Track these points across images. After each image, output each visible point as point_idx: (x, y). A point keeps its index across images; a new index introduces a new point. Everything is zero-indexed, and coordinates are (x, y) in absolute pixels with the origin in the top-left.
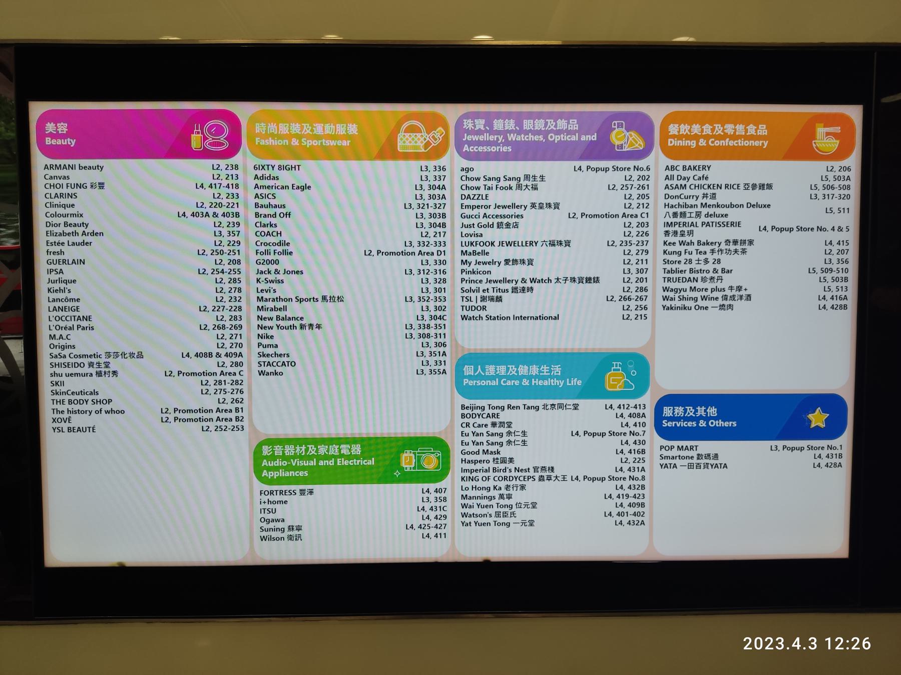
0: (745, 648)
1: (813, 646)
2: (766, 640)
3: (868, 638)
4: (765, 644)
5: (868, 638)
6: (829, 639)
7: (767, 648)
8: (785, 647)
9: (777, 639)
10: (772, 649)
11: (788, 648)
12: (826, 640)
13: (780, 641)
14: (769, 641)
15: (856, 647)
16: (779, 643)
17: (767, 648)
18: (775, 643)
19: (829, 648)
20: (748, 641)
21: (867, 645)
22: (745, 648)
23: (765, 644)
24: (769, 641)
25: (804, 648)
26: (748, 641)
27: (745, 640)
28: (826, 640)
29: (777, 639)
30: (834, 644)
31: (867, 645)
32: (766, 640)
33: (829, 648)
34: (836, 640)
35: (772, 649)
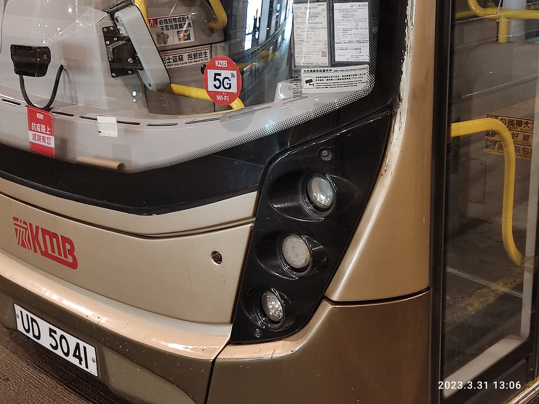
0: (439, 388)
1: (480, 387)
2: (452, 383)
3: (519, 382)
4: (451, 385)
5: (519, 382)
6: (496, 383)
7: (452, 388)
8: (473, 387)
9: (458, 383)
10: (456, 388)
11: (507, 388)
12: (494, 383)
13: (460, 383)
14: (454, 383)
15: (441, 387)
16: (479, 385)
17: (452, 388)
18: (457, 385)
19: (496, 388)
20: (441, 383)
21: (518, 386)
22: (439, 388)
23: (451, 385)
24: (454, 383)
25: (475, 388)
26: (441, 383)
27: (439, 383)
28: (494, 383)
29: (458, 383)
30: (499, 385)
31: (518, 386)
32: (452, 383)
33: (496, 388)
34: (500, 383)
35: (456, 388)
